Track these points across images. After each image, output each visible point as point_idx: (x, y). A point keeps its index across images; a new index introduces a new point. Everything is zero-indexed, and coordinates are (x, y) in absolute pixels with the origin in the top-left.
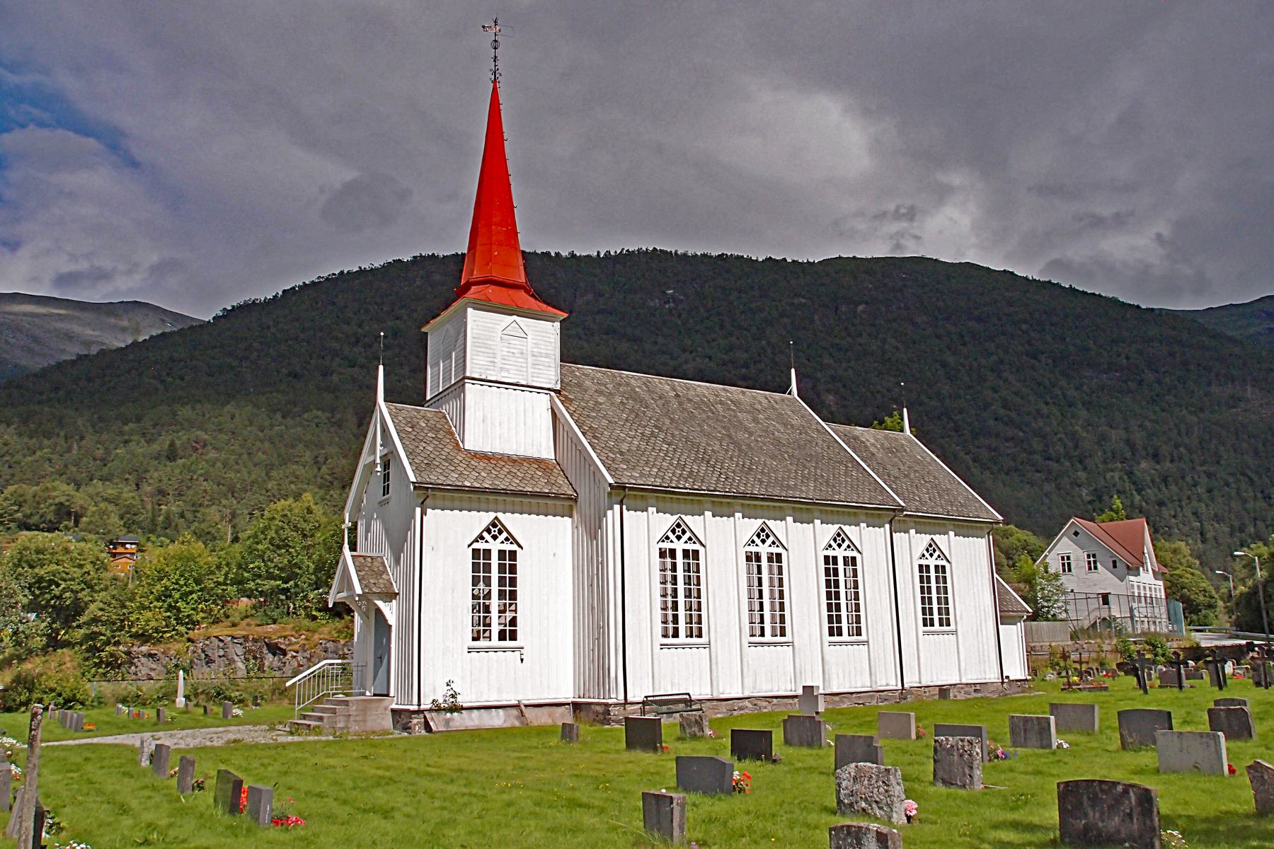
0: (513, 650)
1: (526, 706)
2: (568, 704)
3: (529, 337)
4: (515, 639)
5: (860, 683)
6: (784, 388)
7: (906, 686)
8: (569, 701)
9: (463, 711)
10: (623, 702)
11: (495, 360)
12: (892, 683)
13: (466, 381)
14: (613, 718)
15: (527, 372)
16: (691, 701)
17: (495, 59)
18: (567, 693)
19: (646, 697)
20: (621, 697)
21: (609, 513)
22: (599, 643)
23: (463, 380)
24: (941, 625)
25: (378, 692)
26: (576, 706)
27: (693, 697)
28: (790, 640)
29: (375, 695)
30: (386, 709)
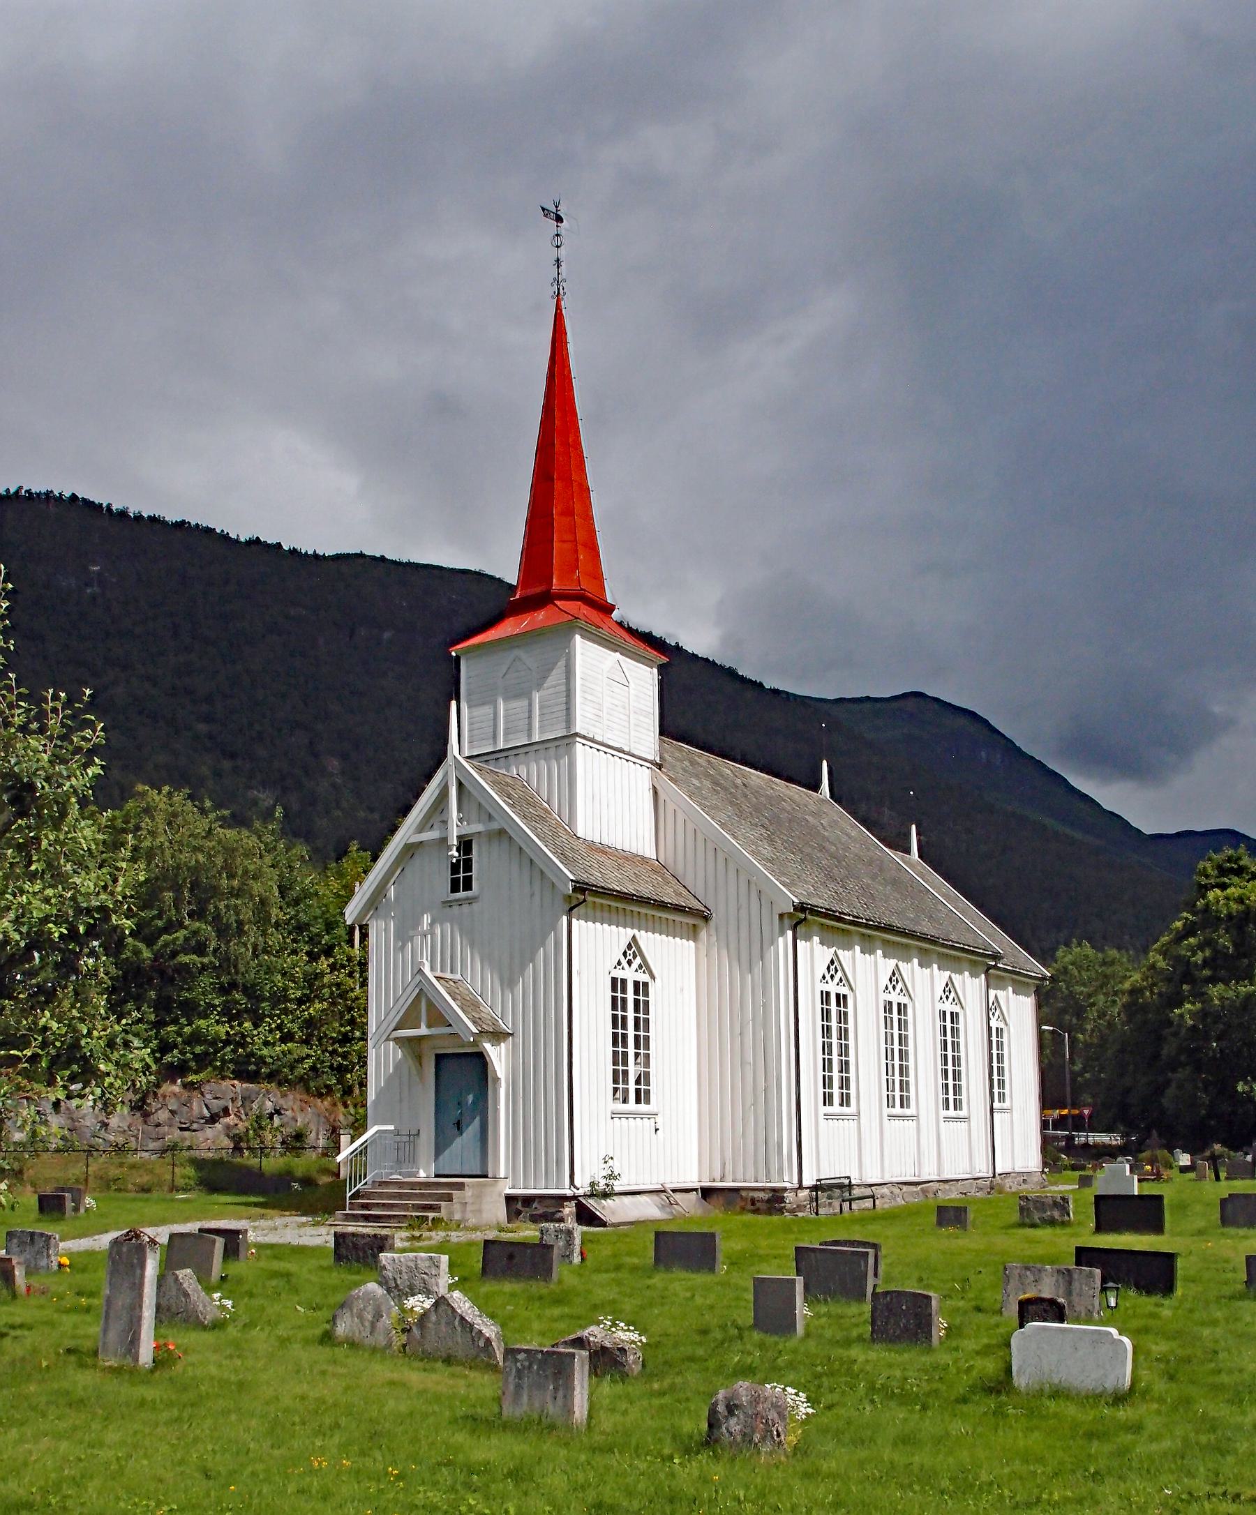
0: (642, 1116)
1: (674, 1191)
2: (696, 1190)
3: (632, 685)
4: (648, 1101)
5: (956, 1168)
6: (815, 787)
7: (998, 1171)
8: (697, 1185)
9: (614, 1198)
10: (797, 1186)
11: (600, 713)
12: (983, 1169)
13: (578, 739)
14: (788, 1206)
15: (629, 734)
16: (850, 1186)
17: (558, 262)
18: (692, 1177)
19: (818, 1180)
20: (795, 1180)
21: (781, 939)
22: (755, 1110)
23: (570, 738)
24: (638, 1101)
25: (441, 1172)
26: (707, 1193)
27: (853, 1182)
28: (914, 1113)
29: (437, 1176)
30: (500, 1195)
